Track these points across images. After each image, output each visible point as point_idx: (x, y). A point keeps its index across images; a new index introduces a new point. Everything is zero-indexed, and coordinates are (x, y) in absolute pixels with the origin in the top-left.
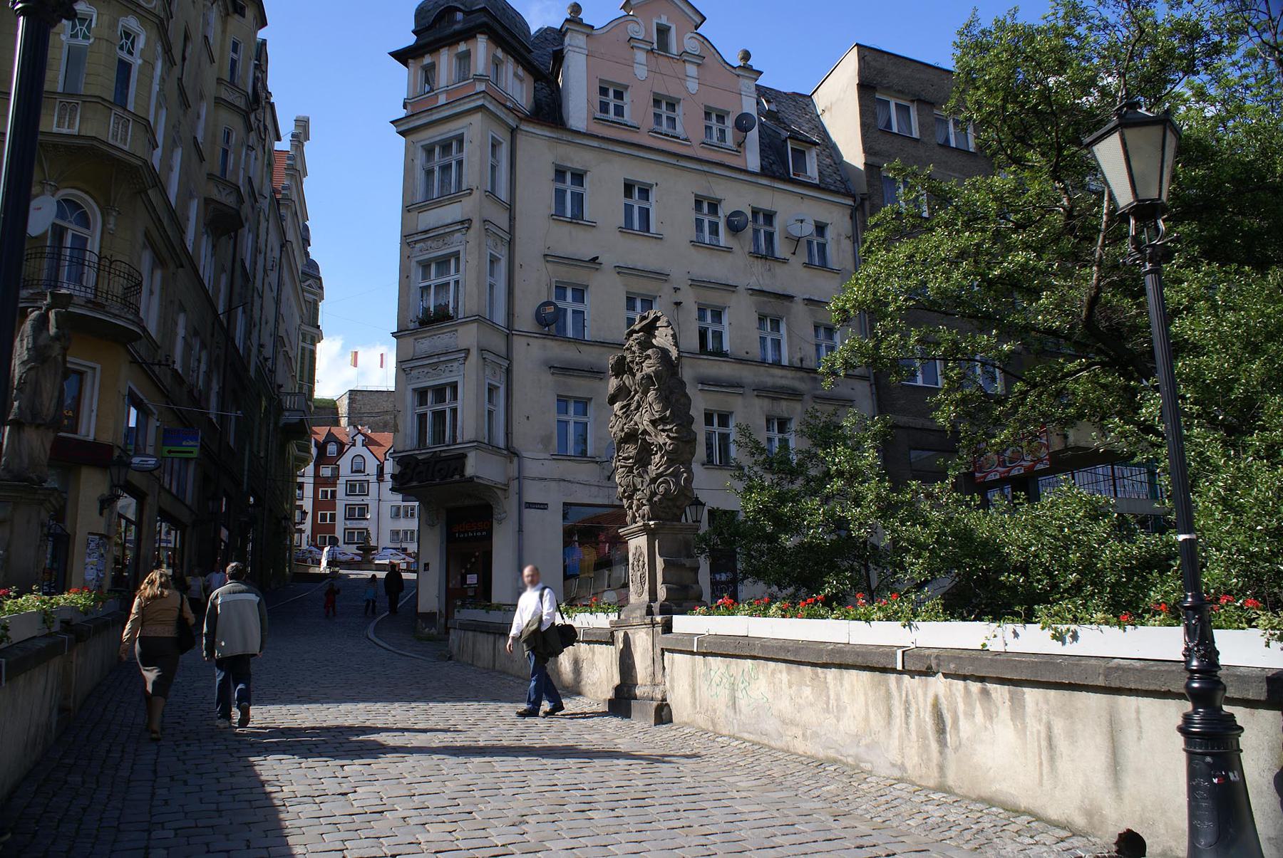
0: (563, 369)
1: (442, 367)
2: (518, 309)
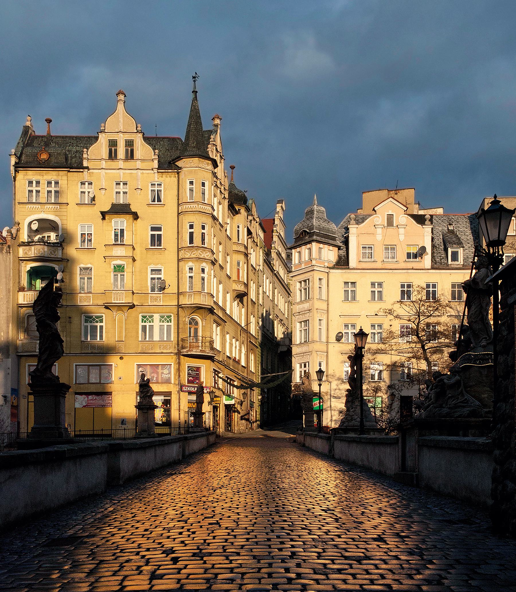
2: (330, 336)
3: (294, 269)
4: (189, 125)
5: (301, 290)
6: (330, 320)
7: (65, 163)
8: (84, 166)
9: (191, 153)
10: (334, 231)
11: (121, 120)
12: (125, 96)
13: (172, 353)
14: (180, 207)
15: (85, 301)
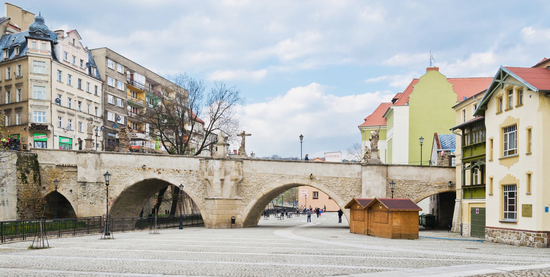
0: (59, 112)
2: (52, 99)
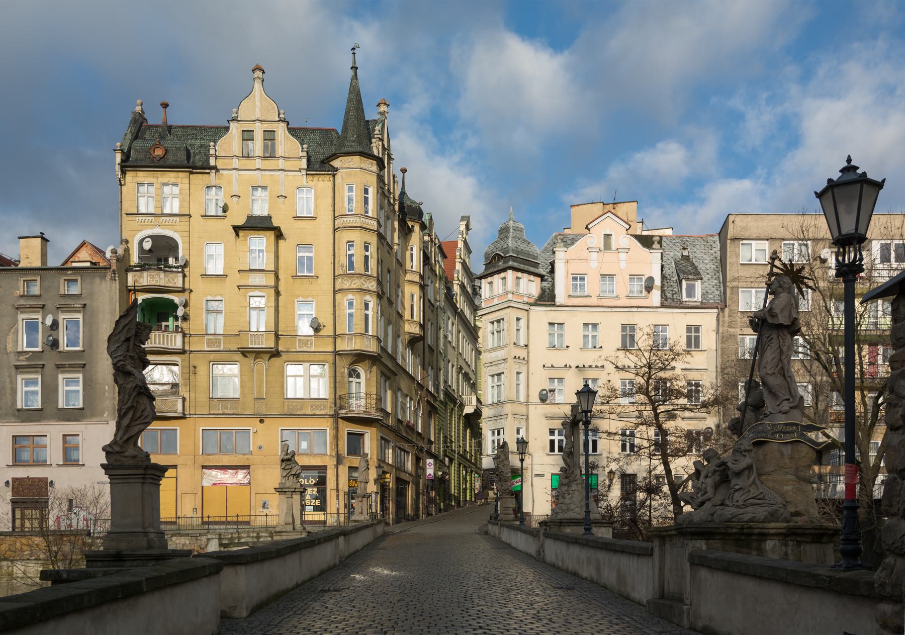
1: (498, 421)
3: (485, 305)
4: (347, 112)
5: (493, 333)
6: (530, 373)
7: (186, 162)
8: (211, 165)
9: (350, 150)
10: (536, 255)
11: (258, 104)
12: (264, 72)
13: (326, 415)
14: (336, 221)
15: (214, 345)
